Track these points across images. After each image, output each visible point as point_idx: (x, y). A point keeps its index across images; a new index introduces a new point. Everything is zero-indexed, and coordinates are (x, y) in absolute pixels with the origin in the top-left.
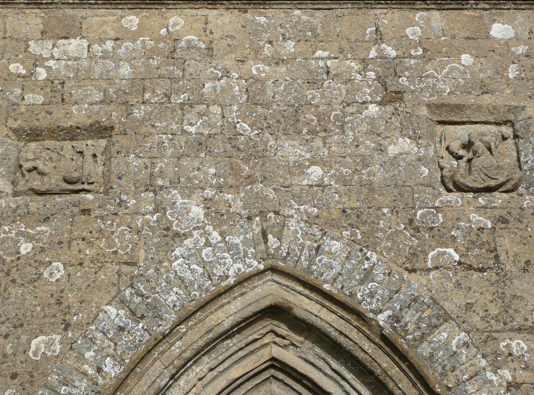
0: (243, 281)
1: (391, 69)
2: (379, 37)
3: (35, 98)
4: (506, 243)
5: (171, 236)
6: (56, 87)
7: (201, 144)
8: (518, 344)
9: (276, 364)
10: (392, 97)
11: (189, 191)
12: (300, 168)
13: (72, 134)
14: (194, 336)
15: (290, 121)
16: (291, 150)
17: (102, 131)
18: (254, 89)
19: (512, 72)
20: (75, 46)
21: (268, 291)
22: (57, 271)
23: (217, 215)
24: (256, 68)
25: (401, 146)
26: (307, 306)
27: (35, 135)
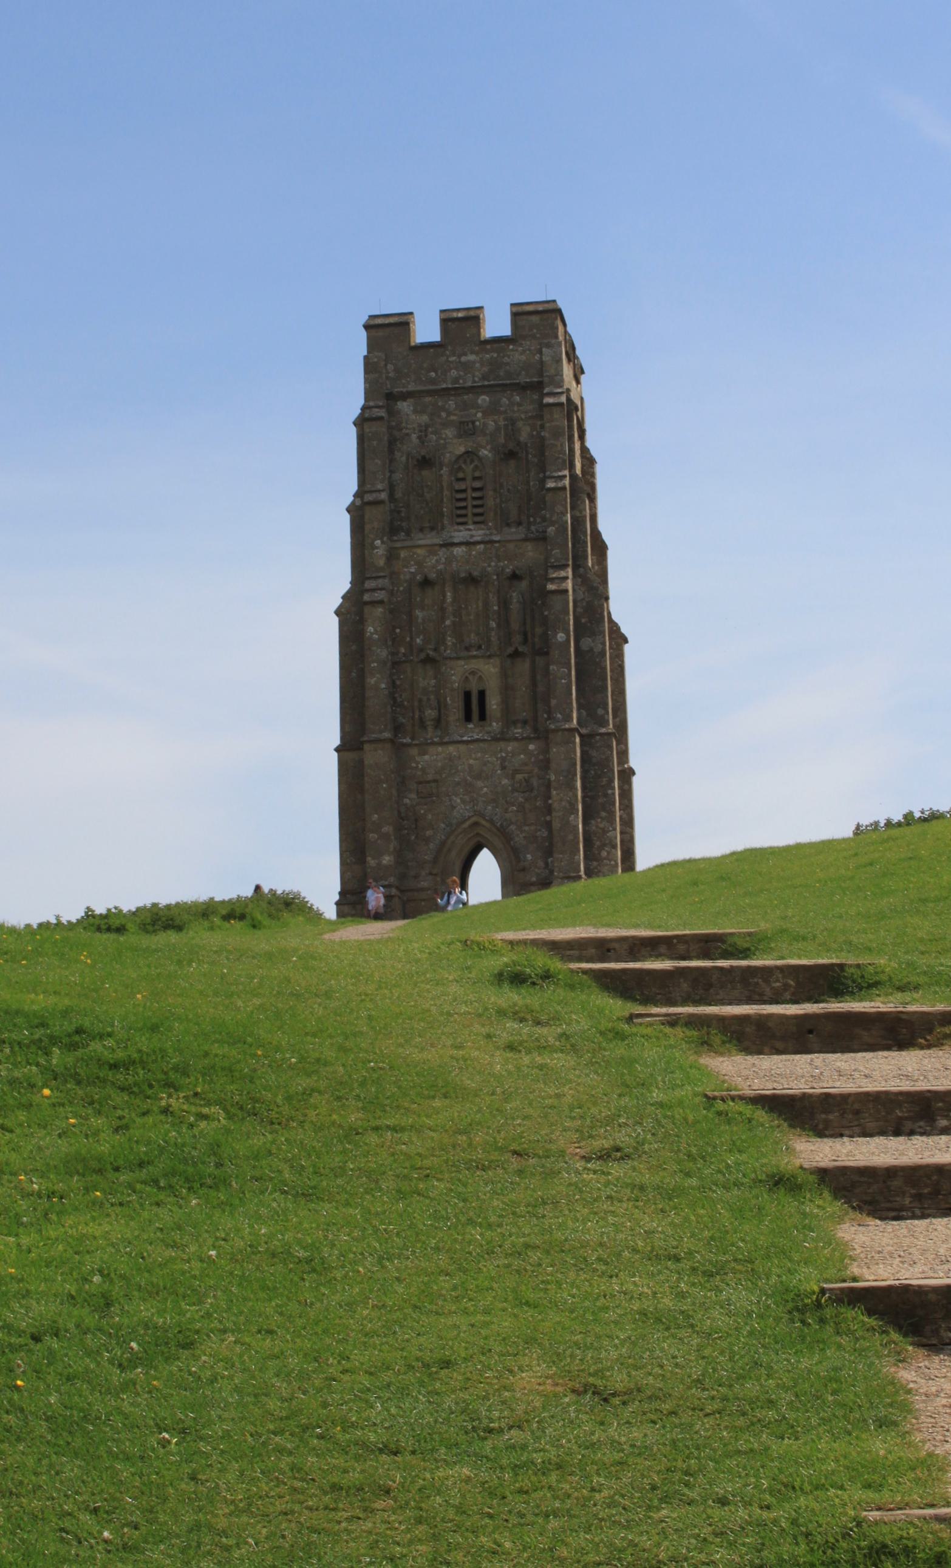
0: (469, 817)
1: (503, 759)
2: (501, 751)
3: (419, 773)
4: (527, 805)
5: (454, 808)
6: (423, 770)
7: (458, 783)
8: (527, 828)
9: (478, 834)
10: (503, 768)
11: (457, 795)
12: (482, 788)
13: (428, 782)
14: (460, 830)
15: (478, 777)
16: (480, 784)
17: (435, 781)
18: (470, 766)
19: (533, 759)
20: (426, 757)
21: (474, 819)
22: (430, 817)
23: (463, 801)
24: (471, 762)
25: (505, 781)
26: (484, 822)
27: (420, 783)
